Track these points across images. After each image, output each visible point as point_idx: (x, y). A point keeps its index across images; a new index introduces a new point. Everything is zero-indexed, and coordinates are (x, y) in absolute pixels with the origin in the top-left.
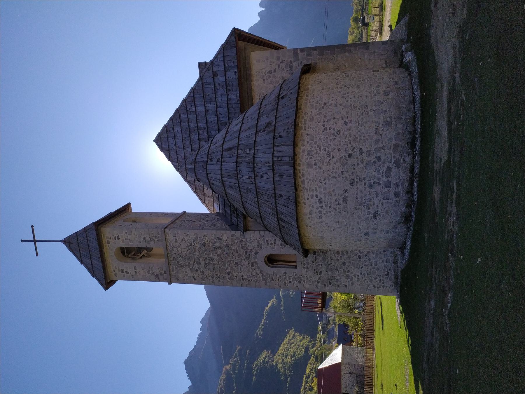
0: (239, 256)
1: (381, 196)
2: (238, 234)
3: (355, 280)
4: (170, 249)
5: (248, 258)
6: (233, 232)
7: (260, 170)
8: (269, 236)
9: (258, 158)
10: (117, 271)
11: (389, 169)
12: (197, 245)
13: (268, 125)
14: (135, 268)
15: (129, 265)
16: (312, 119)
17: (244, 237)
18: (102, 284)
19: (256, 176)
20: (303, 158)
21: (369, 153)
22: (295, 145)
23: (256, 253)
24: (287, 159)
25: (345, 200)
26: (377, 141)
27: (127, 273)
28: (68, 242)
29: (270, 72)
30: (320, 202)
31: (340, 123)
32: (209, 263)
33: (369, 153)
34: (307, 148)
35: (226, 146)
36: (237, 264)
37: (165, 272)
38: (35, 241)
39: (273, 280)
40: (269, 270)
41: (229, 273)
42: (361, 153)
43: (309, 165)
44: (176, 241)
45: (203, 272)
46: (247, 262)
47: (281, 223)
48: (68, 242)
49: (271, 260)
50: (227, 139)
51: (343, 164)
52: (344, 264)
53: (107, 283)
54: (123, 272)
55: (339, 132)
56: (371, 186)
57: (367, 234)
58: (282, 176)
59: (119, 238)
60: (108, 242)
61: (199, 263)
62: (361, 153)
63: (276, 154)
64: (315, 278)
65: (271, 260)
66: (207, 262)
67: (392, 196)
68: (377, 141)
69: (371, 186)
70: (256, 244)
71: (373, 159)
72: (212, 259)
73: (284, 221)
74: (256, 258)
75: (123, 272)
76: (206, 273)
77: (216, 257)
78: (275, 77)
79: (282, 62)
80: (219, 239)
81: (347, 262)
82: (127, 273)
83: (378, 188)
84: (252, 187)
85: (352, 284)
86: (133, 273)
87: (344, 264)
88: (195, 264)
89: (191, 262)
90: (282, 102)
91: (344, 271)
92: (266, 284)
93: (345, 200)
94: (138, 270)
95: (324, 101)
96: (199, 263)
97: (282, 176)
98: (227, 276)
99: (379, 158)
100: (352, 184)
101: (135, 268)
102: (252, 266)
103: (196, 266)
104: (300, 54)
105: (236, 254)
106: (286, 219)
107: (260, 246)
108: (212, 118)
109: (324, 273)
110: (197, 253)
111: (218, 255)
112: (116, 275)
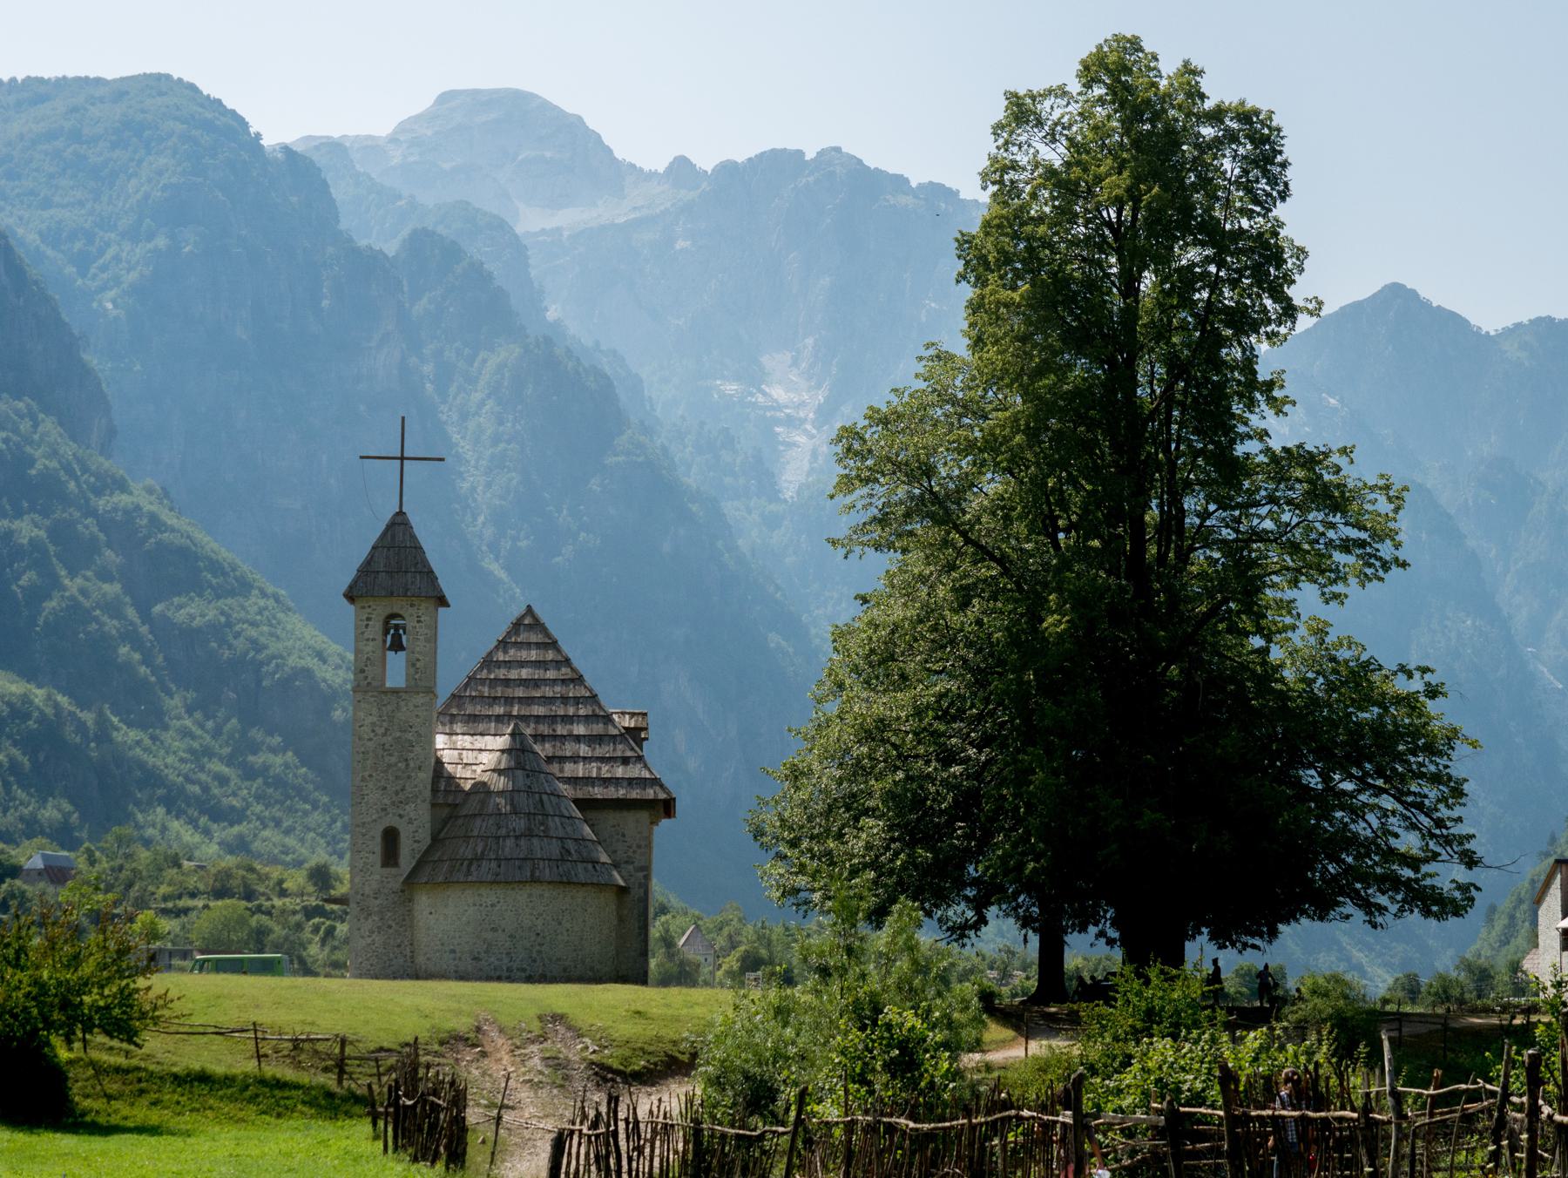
0: (397, 793)
1: (497, 963)
2: (428, 793)
3: (369, 940)
4: (404, 696)
5: (393, 803)
6: (429, 787)
7: (523, 842)
8: (425, 839)
9: (535, 841)
10: (369, 610)
11: (524, 970)
12: (409, 736)
13: (568, 852)
14: (373, 640)
15: (376, 626)
16: (572, 898)
17: (424, 801)
18: (351, 587)
19: (517, 837)
20: (537, 890)
21: (539, 952)
22: (549, 883)
23: (401, 816)
24: (537, 874)
25: (494, 930)
26: (550, 960)
27: (367, 626)
28: (399, 523)
29: (624, 835)
30: (492, 905)
31: (568, 926)
32: (384, 750)
33: (539, 952)
34: (547, 895)
35: (545, 797)
36: (385, 788)
37: (369, 684)
38: (402, 458)
39: (364, 835)
40: (378, 832)
41: (370, 776)
42: (540, 945)
43: (530, 895)
44: (416, 706)
45: (370, 740)
46: (386, 801)
47: (466, 863)
48: (399, 523)
49: (391, 838)
50: (552, 798)
51: (530, 928)
52: (390, 927)
53: (351, 596)
54: (368, 619)
55: (560, 924)
56: (508, 954)
57: (453, 951)
58: (519, 868)
59: (419, 622)
60: (412, 605)
61: (384, 735)
62: (540, 945)
63: (541, 863)
64: (367, 890)
65: (391, 838)
66: (387, 746)
67: (498, 973)
68: (550, 960)
69: (508, 954)
70: (412, 815)
71: (534, 955)
72: (391, 755)
73: (470, 865)
74: (394, 814)
75: (368, 619)
76: (369, 744)
77: (393, 760)
78: (618, 840)
79: (634, 852)
80: (420, 768)
81: (391, 931)
82: (367, 626)
83: (506, 960)
84: (503, 832)
85: (363, 937)
86: (366, 636)
87: (390, 927)
88: (383, 730)
89: (385, 724)
90: (590, 866)
91: (379, 928)
92: (358, 826)
93: (494, 930)
94: (371, 643)
95: (589, 910)
96: (384, 735)
97: (519, 868)
98: (367, 774)
99: (535, 961)
100: (511, 936)
101: (373, 640)
102: (384, 810)
103: (380, 731)
104: (641, 874)
105: (398, 788)
106: (473, 868)
107: (410, 822)
108: (569, 749)
109: (378, 902)
110: (398, 734)
111: (396, 764)
112: (363, 608)
